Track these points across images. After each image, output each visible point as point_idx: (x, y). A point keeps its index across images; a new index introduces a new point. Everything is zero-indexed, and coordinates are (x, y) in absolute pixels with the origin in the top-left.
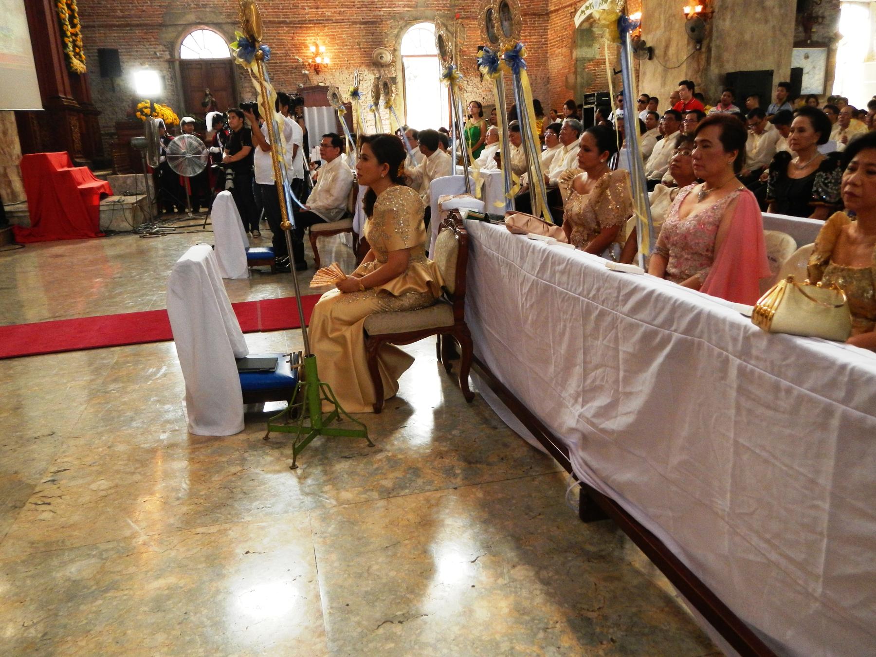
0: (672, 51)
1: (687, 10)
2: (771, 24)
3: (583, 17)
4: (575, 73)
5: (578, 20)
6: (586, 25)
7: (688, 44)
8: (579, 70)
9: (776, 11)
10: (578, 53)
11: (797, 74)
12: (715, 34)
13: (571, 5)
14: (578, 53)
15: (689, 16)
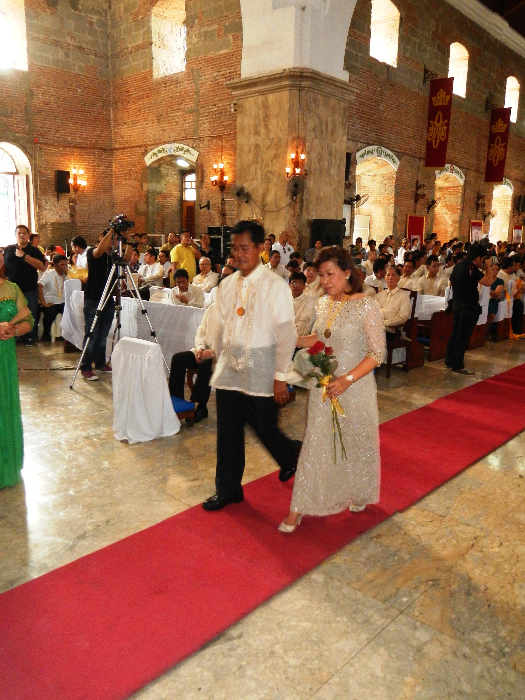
0: (270, 198)
1: (288, 170)
2: (333, 186)
3: (155, 158)
4: (147, 202)
5: (149, 160)
6: (156, 165)
7: (287, 195)
8: (150, 200)
9: (336, 178)
10: (146, 187)
11: (344, 221)
12: (306, 191)
13: (140, 147)
14: (146, 187)
15: (289, 175)
